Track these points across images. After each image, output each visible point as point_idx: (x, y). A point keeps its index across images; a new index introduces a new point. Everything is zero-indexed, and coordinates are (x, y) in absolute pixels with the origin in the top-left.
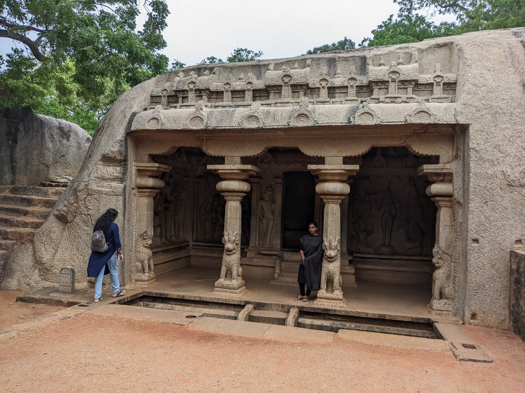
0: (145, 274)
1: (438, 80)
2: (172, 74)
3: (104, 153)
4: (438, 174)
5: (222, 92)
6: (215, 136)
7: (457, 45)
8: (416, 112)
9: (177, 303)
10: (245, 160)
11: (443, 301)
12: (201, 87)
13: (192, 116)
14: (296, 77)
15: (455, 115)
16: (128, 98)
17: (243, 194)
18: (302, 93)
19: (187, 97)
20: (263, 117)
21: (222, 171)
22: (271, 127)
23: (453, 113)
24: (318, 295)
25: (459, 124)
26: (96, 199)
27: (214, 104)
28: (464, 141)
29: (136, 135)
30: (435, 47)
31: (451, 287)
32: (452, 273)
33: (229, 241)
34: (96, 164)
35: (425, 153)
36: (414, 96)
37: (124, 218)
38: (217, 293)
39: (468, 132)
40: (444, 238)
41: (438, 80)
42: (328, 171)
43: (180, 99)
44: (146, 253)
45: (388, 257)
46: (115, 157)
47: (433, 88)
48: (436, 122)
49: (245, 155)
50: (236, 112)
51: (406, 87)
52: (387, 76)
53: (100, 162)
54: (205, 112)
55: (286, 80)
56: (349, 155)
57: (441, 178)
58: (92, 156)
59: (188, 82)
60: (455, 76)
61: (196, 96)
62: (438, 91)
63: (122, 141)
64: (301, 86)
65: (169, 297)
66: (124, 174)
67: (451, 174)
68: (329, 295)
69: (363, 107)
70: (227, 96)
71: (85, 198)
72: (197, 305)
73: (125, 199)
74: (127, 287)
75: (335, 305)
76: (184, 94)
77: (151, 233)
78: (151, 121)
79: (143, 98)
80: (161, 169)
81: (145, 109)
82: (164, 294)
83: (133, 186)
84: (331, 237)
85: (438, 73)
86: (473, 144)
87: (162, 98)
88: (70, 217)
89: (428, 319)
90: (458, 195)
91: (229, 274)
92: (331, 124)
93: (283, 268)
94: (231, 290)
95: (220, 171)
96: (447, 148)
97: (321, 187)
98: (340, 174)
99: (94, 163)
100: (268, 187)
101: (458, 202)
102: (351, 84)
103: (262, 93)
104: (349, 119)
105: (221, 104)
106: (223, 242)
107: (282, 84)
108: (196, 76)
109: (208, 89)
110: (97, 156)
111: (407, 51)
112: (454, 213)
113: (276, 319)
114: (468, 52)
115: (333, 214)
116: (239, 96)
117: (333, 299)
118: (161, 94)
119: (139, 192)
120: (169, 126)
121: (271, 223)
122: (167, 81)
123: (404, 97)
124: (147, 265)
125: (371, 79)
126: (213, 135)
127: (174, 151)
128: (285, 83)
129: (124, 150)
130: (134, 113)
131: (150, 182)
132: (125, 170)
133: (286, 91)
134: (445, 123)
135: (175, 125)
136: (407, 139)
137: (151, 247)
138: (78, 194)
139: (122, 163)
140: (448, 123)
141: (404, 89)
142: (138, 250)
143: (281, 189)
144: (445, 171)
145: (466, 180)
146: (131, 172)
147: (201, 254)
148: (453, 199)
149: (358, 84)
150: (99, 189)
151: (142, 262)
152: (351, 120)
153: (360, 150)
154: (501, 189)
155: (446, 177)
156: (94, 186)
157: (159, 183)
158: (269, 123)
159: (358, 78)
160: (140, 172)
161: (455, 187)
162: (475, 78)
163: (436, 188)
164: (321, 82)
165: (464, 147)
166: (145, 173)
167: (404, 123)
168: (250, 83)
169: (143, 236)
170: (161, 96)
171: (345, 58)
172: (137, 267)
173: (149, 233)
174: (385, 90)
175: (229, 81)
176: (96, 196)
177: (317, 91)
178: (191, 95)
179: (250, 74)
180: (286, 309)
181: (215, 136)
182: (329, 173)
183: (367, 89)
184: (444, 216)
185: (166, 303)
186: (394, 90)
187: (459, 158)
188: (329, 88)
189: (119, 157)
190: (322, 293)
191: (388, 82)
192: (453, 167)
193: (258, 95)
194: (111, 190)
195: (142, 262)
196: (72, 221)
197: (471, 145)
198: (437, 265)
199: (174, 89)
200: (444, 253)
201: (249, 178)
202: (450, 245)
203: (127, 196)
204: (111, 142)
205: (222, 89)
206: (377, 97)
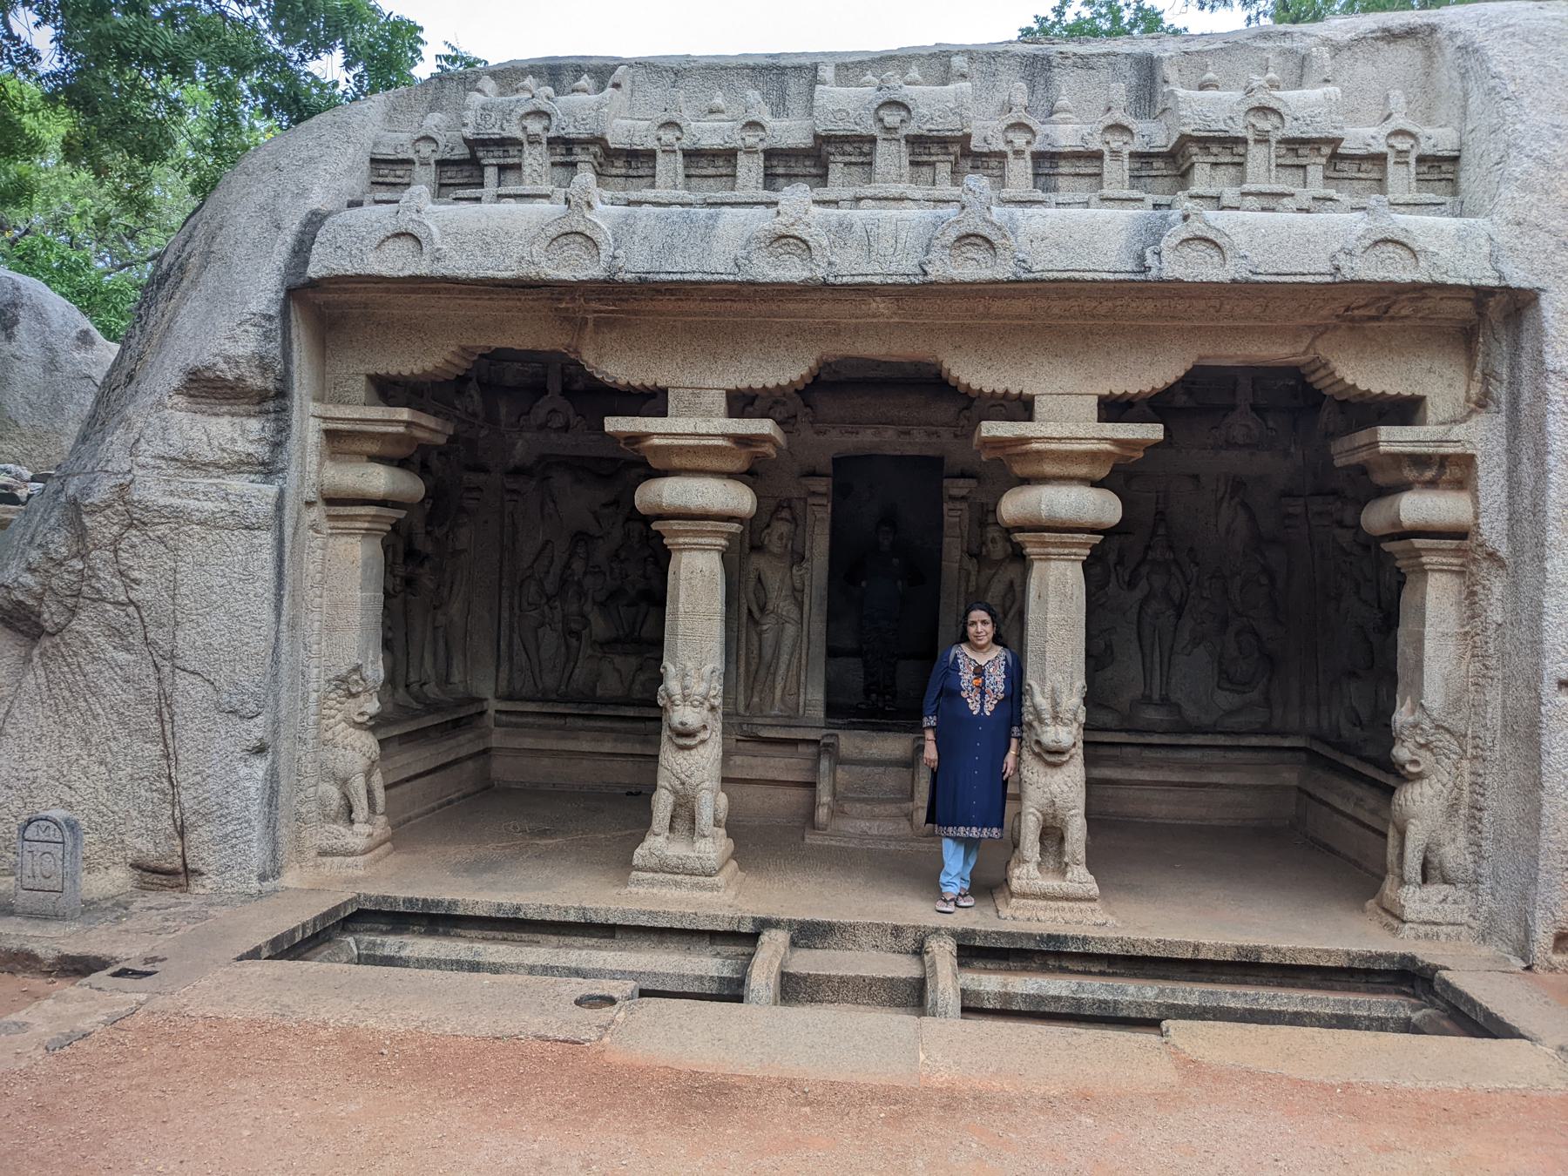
0: (356, 827)
1: (1402, 144)
2: (448, 84)
3: (193, 361)
5: (650, 155)
6: (636, 313)
7: (1452, 35)
8: (1367, 242)
9: (491, 934)
10: (741, 403)
11: (1435, 891)
12: (572, 130)
13: (553, 231)
14: (924, 111)
15: (1493, 258)
16: (284, 162)
17: (734, 527)
18: (944, 170)
19: (518, 167)
20: (825, 243)
21: (663, 442)
23: (1486, 249)
24: (1015, 885)
25: (1507, 288)
26: (161, 540)
27: (621, 194)
28: (1516, 348)
29: (321, 298)
30: (1377, 39)
31: (1462, 841)
32: (1466, 793)
33: (685, 697)
34: (160, 404)
35: (1376, 389)
36: (1332, 193)
37: (279, 616)
38: (642, 891)
39: (1539, 318)
40: (1438, 678)
41: (1402, 144)
42: (1053, 446)
43: (491, 174)
44: (356, 750)
45: (1166, 740)
46: (239, 379)
47: (1384, 170)
48: (1438, 277)
49: (744, 385)
50: (720, 223)
51: (1303, 161)
52: (1241, 123)
53: (176, 399)
54: (604, 217)
55: (892, 118)
56: (1118, 391)
57: (1429, 474)
58: (139, 376)
59: (522, 112)
60: (1455, 136)
61: (553, 164)
62: (1400, 179)
63: (269, 318)
64: (943, 142)
65: (460, 911)
66: (277, 446)
67: (1468, 461)
68: (1051, 883)
69: (1186, 218)
70: (669, 168)
71: (117, 539)
72: (568, 940)
73: (280, 542)
74: (290, 879)
75: (1079, 917)
76: (506, 154)
77: (376, 671)
78: (389, 245)
79: (345, 163)
80: (419, 433)
81: (353, 204)
82: (438, 903)
83: (311, 495)
84: (1055, 679)
85: (1399, 122)
86: (1557, 356)
87: (417, 168)
88: (51, 615)
89: (1403, 957)
90: (1493, 531)
91: (685, 818)
92: (1077, 275)
93: (840, 788)
94: (695, 879)
95: (656, 441)
96: (1449, 373)
97: (1015, 505)
98: (1093, 456)
99: (150, 400)
100: (779, 507)
101: (1492, 556)
102: (1114, 145)
103: (812, 160)
104: (1141, 257)
105: (649, 194)
106: (661, 702)
107: (875, 131)
108: (550, 90)
109: (599, 141)
110: (165, 375)
111: (1287, 44)
112: (1473, 593)
113: (884, 980)
114: (1499, 54)
115: (1058, 595)
116: (711, 171)
117: (1067, 898)
118: (411, 155)
119: (330, 517)
120: (460, 265)
121: (790, 630)
122: (432, 109)
123: (1304, 196)
124: (363, 792)
125: (1187, 130)
126: (625, 306)
127: (465, 365)
128: (888, 129)
129: (277, 352)
130: (314, 213)
131: (379, 480)
132: (280, 431)
133: (891, 157)
134: (1463, 281)
135: (488, 262)
137: (375, 724)
138: (87, 520)
139: (270, 405)
140: (1475, 282)
141: (1294, 170)
142: (329, 735)
143: (824, 514)
144: (1451, 450)
145: (1529, 482)
146: (302, 440)
147: (607, 747)
149: (1138, 145)
150: (176, 501)
151: (344, 782)
152: (1149, 262)
155: (1452, 471)
156: (152, 491)
157: (409, 486)
158: (850, 266)
159: (1137, 126)
160: (337, 440)
161: (1483, 504)
162: (1538, 137)
163: (1417, 507)
164: (1011, 136)
165: (1514, 367)
166: (356, 447)
167: (1329, 279)
168: (753, 125)
169: (345, 685)
170: (410, 162)
171: (1082, 57)
172: (322, 803)
173: (368, 672)
174: (1232, 170)
175: (674, 116)
176: (162, 530)
177: (993, 163)
178: (535, 160)
179: (753, 95)
180: (909, 942)
181: (636, 313)
182: (1052, 452)
183: (1172, 163)
184: (1437, 602)
185: (446, 934)
186: (1263, 169)
187: (1493, 408)
188: (1038, 157)
189: (256, 382)
190: (1027, 874)
191: (1244, 141)
192: (1481, 436)
193: (780, 171)
194: (224, 506)
195: (344, 782)
196: (60, 630)
197: (1551, 361)
198: (1412, 769)
199: (468, 132)
200: (1438, 727)
202: (1459, 700)
203: (288, 531)
204: (223, 323)
205: (651, 144)
206: (1212, 192)
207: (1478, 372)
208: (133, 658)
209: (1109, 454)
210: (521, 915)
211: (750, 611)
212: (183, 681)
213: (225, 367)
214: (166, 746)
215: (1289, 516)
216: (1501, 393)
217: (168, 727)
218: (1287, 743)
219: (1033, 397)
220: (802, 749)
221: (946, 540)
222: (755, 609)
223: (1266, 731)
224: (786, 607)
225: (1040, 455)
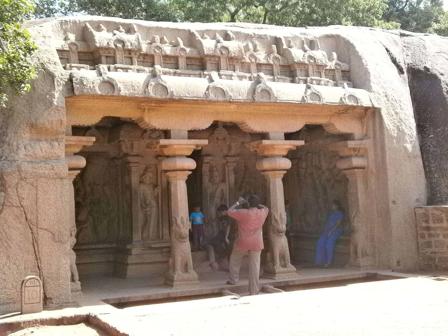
14: (232, 50)
90: (372, 167)
95: (175, 147)
136: (331, 117)
154: (404, 160)
157: (82, 162)
190: (278, 268)
192: (368, 143)
201: (196, 155)
208: (21, 226)
210: (151, 298)
211: (141, 204)
213: (48, 124)
214: (36, 256)
216: (371, 133)
217: (36, 249)
220: (164, 250)
221: (203, 176)
224: (154, 203)
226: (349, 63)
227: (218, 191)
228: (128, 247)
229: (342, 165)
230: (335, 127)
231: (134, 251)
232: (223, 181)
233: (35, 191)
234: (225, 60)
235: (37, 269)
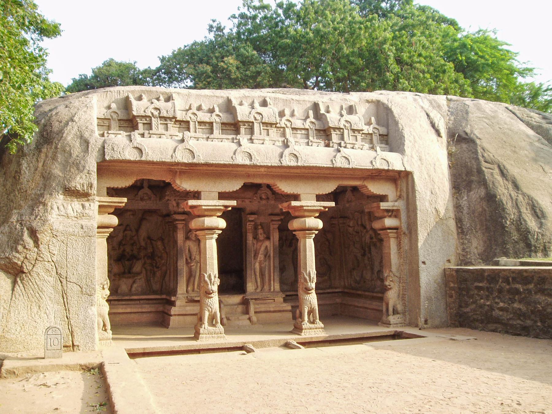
4: (388, 211)
22: (265, 164)
57: (390, 214)
90: (404, 228)
95: (203, 207)
97: (295, 224)
98: (316, 211)
112: (400, 243)
119: (98, 233)
148: (399, 231)
153: (329, 188)
155: (394, 213)
161: (402, 221)
190: (306, 324)
191: (343, 129)
192: (400, 205)
198: (389, 287)
207: (399, 189)
208: (52, 279)
209: (320, 210)
212: (70, 285)
215: (333, 224)
216: (404, 195)
217: (65, 300)
218: (337, 290)
219: (299, 195)
221: (248, 234)
222: (188, 259)
223: (330, 287)
225: (306, 210)
226: (387, 126)
227: (263, 248)
228: (173, 299)
229: (376, 225)
230: (368, 189)
231: (178, 303)
232: (268, 238)
233: (65, 248)
234: (258, 125)
235: (66, 318)
